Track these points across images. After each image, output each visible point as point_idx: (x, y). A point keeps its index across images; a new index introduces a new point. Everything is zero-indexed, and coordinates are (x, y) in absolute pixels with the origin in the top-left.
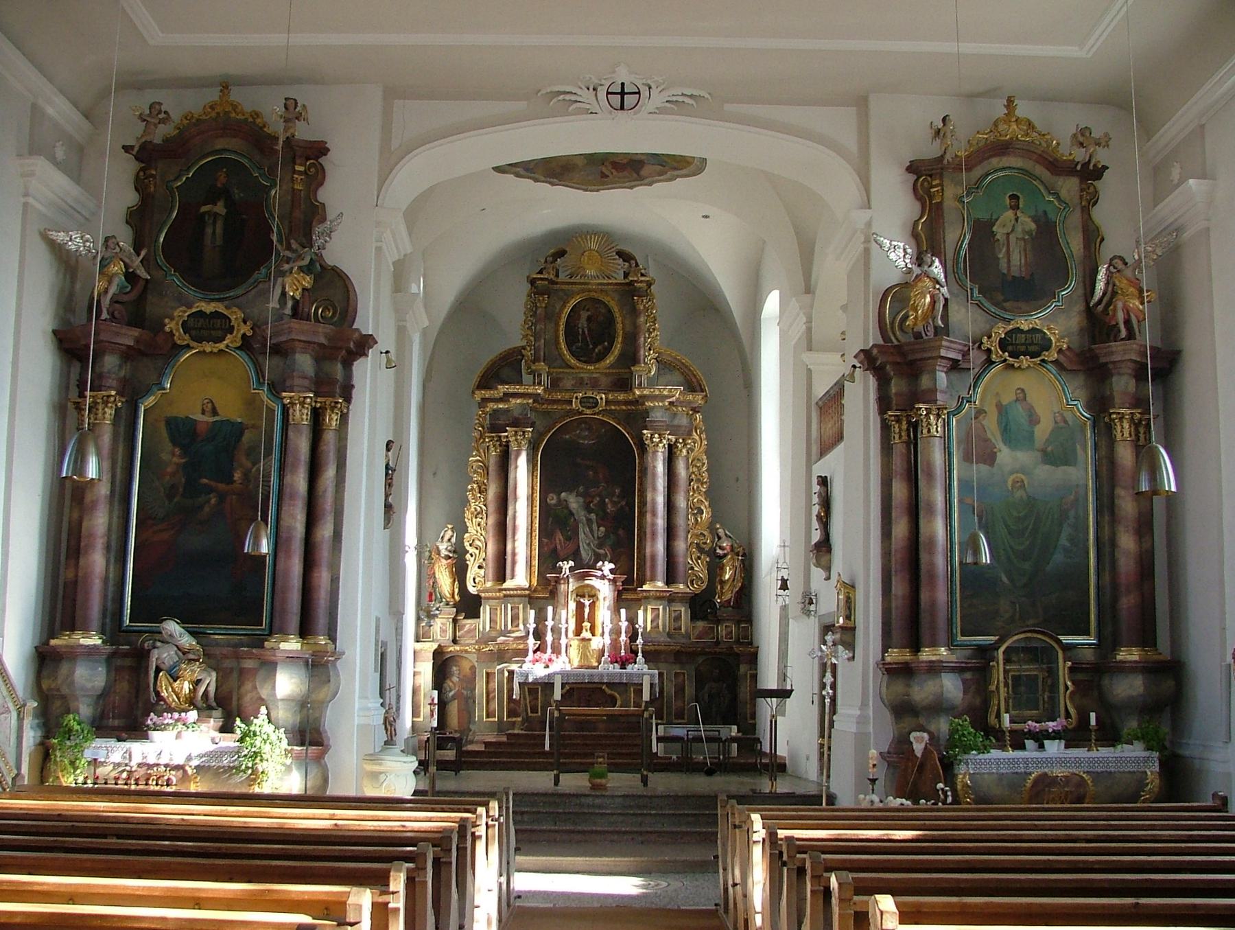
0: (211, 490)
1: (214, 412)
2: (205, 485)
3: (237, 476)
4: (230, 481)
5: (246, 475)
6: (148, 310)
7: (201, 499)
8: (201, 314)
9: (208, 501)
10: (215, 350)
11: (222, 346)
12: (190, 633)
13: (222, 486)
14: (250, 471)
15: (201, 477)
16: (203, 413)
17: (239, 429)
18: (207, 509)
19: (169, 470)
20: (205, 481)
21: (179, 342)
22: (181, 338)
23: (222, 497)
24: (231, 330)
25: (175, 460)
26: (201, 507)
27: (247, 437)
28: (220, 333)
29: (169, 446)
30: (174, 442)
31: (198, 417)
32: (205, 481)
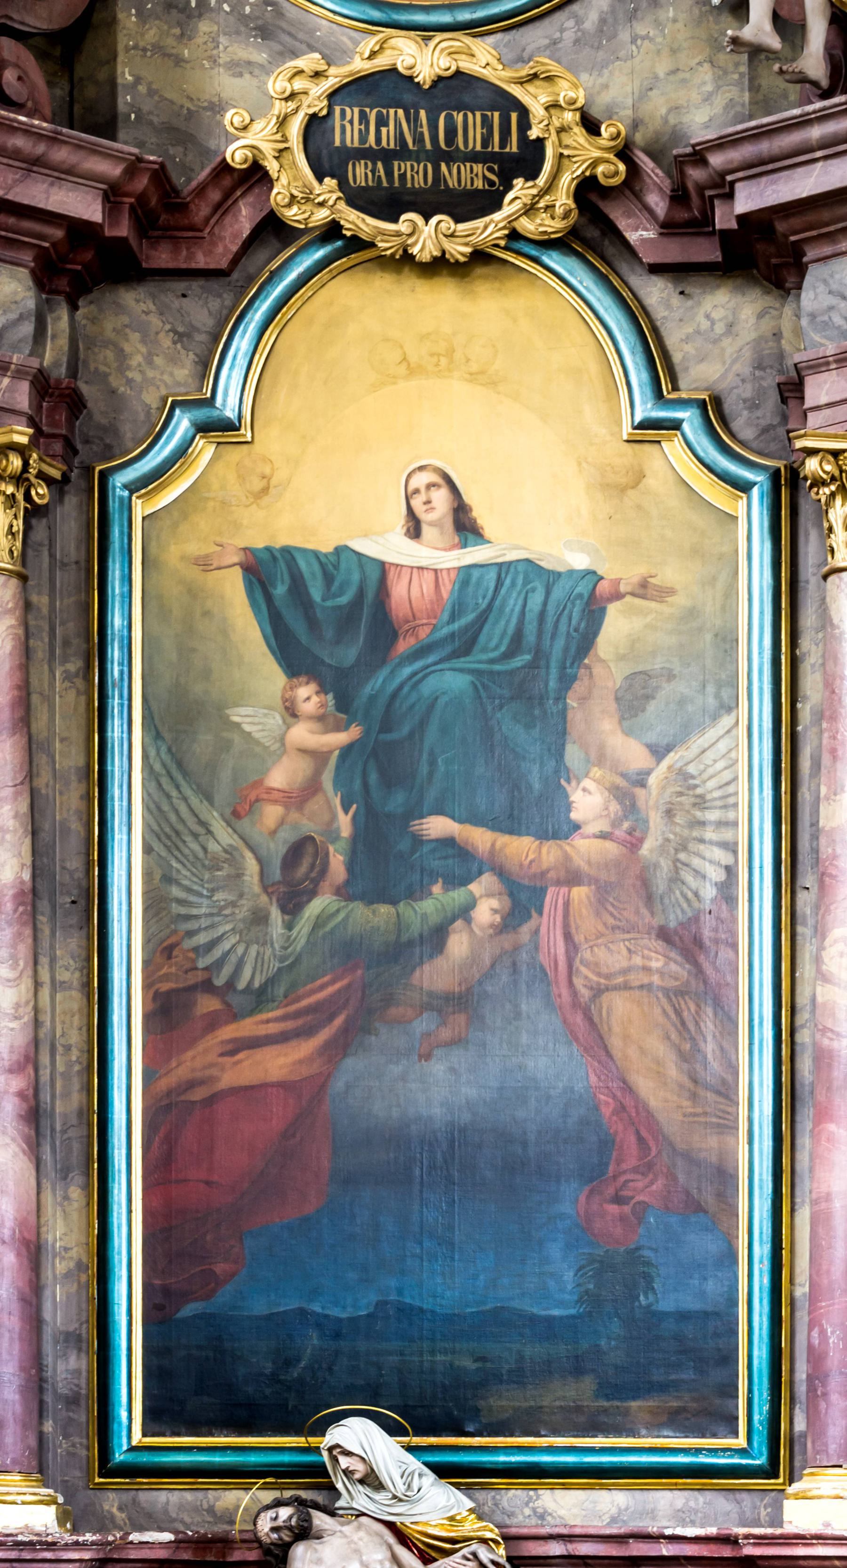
0: (460, 863)
1: (465, 525)
2: (449, 842)
3: (587, 801)
4: (557, 826)
5: (627, 791)
6: (126, 76)
7: (438, 899)
8: (381, 87)
9: (465, 912)
10: (459, 250)
11: (488, 229)
12: (443, 1472)
13: (520, 848)
14: (641, 781)
15: (416, 812)
16: (414, 528)
17: (589, 602)
18: (458, 944)
19: (279, 777)
20: (437, 826)
21: (292, 214)
22: (301, 194)
23: (523, 898)
24: (528, 160)
25: (302, 734)
26: (436, 937)
27: (617, 626)
28: (474, 177)
29: (270, 676)
30: (293, 658)
31: (389, 545)
32: (437, 826)
